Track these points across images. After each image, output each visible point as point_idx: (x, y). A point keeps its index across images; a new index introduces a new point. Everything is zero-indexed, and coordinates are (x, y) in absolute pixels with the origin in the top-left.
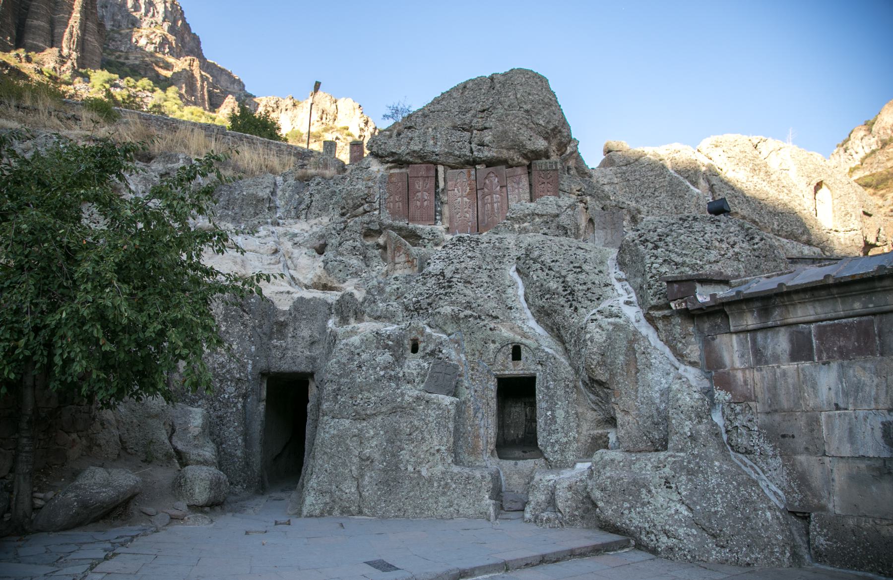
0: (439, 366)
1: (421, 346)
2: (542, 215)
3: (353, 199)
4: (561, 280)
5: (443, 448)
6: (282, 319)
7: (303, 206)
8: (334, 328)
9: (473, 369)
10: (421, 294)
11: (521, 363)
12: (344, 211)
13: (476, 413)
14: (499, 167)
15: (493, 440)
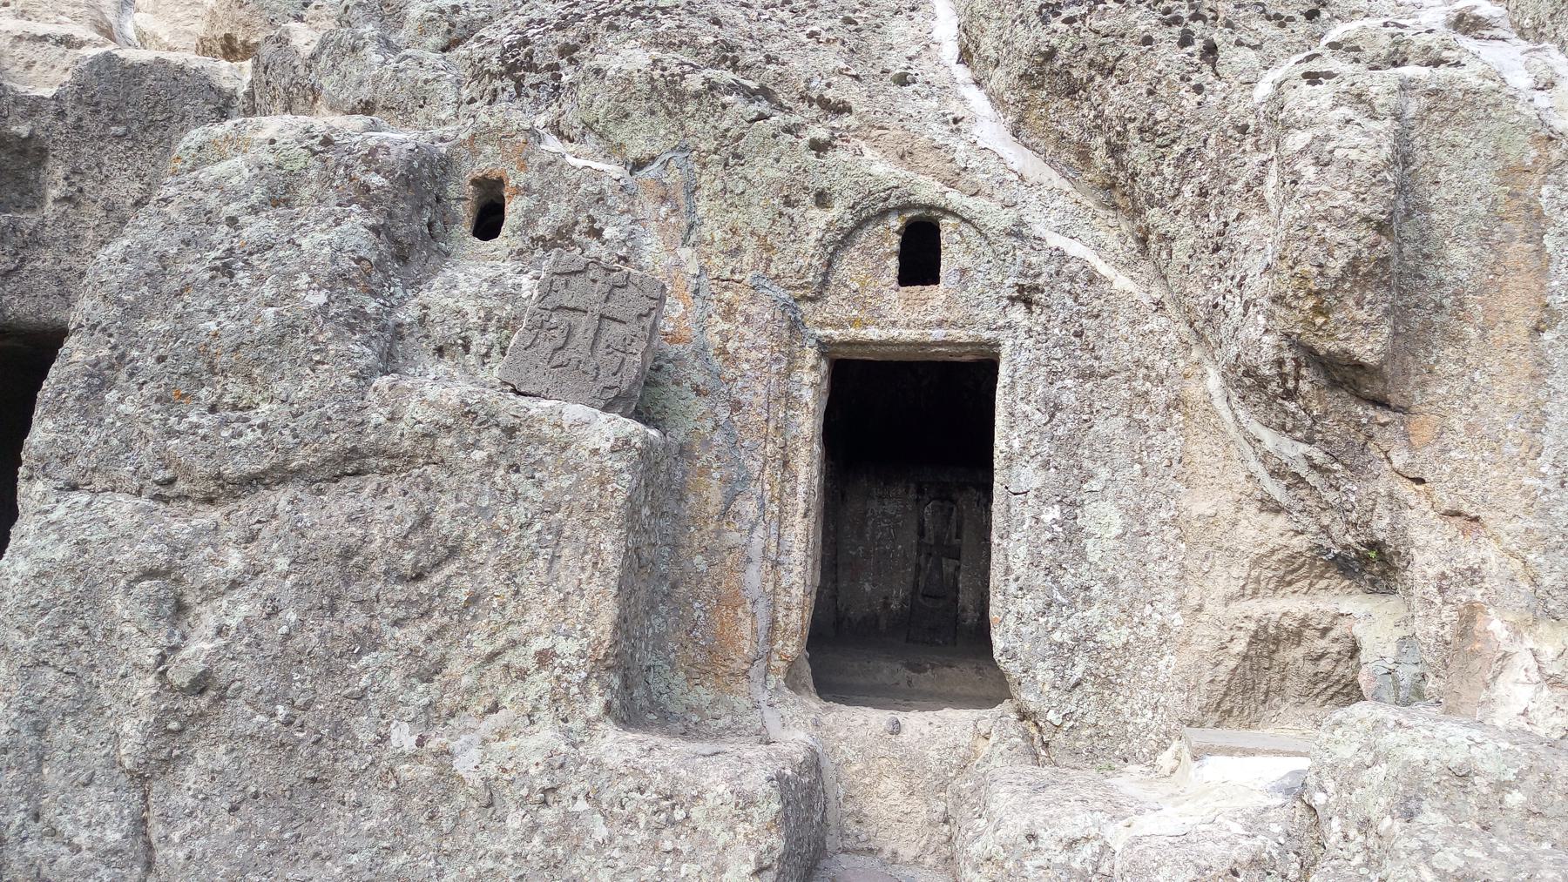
0: (577, 282)
1: (514, 210)
5: (567, 648)
6: (23, 130)
9: (728, 315)
11: (935, 295)
13: (730, 499)
15: (796, 618)
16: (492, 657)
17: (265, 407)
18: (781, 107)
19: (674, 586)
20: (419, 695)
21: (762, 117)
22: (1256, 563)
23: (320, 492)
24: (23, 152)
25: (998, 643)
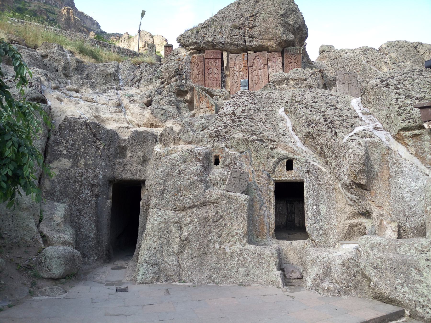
0: (235, 173)
1: (221, 160)
2: (295, 80)
3: (169, 72)
4: (322, 114)
5: (240, 232)
6: (123, 145)
7: (136, 80)
8: (159, 150)
9: (258, 176)
10: (220, 126)
11: (293, 172)
12: (163, 80)
13: (261, 207)
14: (263, 52)
15: (273, 226)
16: (229, 234)
17: (189, 196)
18: (265, 142)
19: (253, 221)
20: (219, 240)
21: (262, 144)
22: (349, 214)
23: (200, 209)
24: (123, 149)
25: (307, 229)
